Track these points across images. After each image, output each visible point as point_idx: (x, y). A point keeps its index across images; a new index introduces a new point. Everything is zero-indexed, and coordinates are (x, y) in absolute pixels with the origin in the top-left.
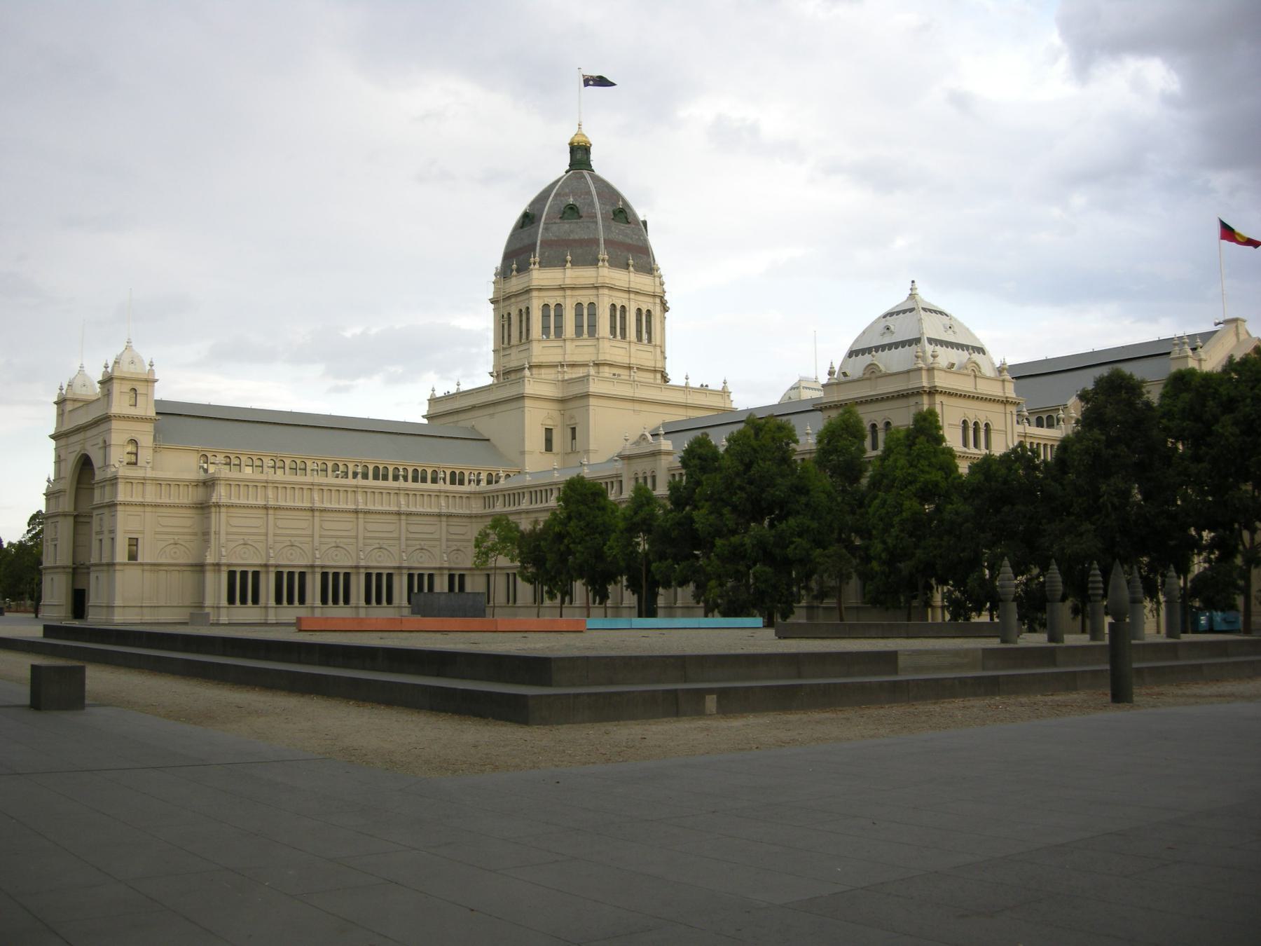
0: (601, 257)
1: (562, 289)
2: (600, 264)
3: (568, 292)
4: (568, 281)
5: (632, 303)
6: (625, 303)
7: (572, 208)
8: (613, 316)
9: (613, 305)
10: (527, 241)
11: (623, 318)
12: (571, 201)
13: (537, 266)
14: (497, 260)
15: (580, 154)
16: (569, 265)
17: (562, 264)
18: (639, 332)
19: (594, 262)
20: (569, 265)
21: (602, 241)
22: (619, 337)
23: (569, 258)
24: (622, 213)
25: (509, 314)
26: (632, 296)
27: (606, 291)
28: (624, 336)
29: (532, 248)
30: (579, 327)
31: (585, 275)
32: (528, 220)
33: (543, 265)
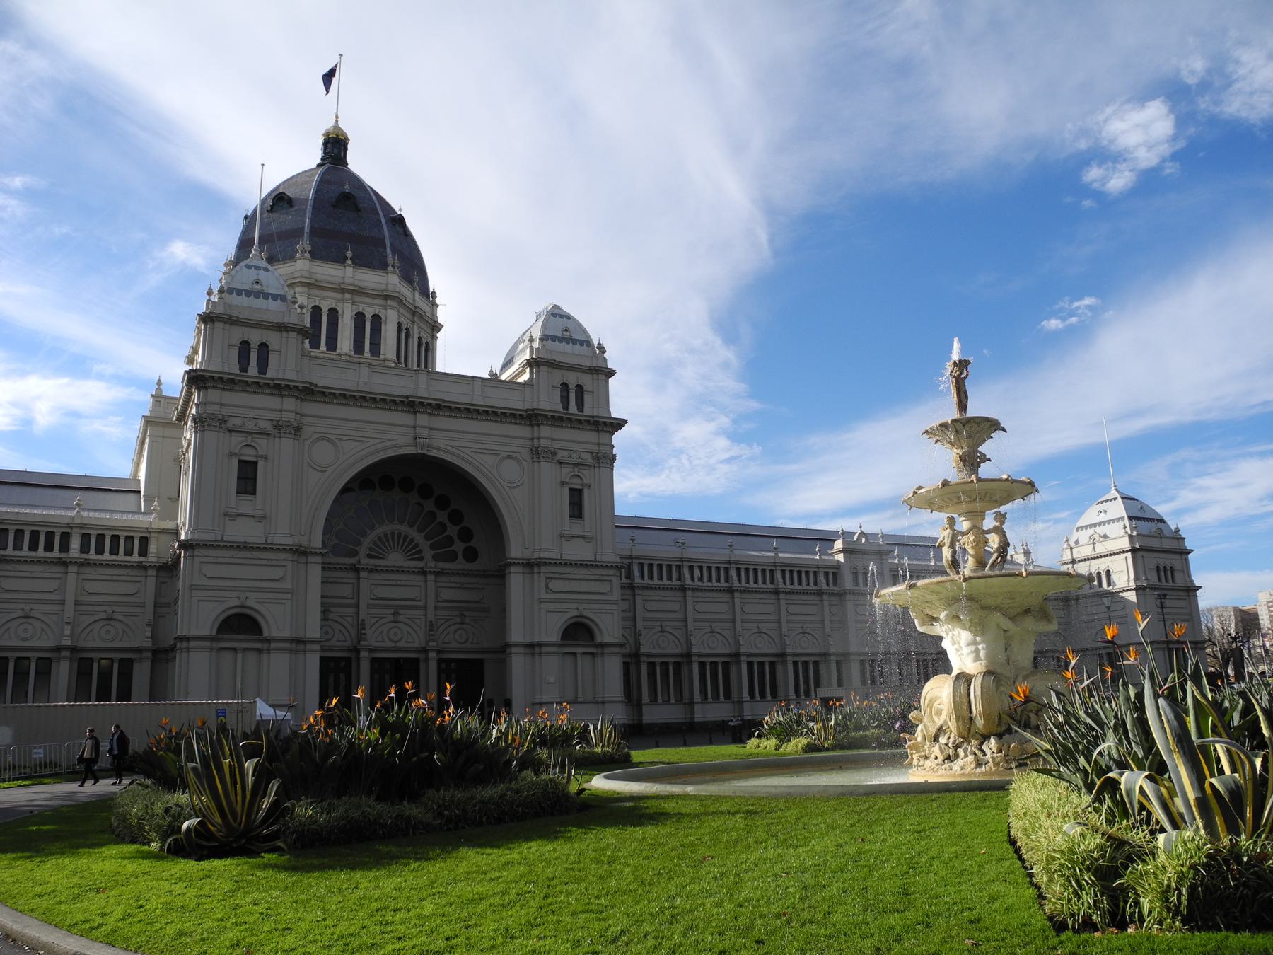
0: (390, 261)
1: (343, 291)
2: (390, 268)
3: (348, 296)
4: (347, 280)
5: (416, 328)
6: (410, 325)
7: (347, 197)
12: (347, 188)
13: (307, 255)
15: (335, 146)
16: (349, 262)
17: (341, 260)
19: (383, 266)
20: (349, 262)
23: (349, 254)
24: (399, 221)
29: (298, 233)
31: (370, 278)
33: (315, 255)
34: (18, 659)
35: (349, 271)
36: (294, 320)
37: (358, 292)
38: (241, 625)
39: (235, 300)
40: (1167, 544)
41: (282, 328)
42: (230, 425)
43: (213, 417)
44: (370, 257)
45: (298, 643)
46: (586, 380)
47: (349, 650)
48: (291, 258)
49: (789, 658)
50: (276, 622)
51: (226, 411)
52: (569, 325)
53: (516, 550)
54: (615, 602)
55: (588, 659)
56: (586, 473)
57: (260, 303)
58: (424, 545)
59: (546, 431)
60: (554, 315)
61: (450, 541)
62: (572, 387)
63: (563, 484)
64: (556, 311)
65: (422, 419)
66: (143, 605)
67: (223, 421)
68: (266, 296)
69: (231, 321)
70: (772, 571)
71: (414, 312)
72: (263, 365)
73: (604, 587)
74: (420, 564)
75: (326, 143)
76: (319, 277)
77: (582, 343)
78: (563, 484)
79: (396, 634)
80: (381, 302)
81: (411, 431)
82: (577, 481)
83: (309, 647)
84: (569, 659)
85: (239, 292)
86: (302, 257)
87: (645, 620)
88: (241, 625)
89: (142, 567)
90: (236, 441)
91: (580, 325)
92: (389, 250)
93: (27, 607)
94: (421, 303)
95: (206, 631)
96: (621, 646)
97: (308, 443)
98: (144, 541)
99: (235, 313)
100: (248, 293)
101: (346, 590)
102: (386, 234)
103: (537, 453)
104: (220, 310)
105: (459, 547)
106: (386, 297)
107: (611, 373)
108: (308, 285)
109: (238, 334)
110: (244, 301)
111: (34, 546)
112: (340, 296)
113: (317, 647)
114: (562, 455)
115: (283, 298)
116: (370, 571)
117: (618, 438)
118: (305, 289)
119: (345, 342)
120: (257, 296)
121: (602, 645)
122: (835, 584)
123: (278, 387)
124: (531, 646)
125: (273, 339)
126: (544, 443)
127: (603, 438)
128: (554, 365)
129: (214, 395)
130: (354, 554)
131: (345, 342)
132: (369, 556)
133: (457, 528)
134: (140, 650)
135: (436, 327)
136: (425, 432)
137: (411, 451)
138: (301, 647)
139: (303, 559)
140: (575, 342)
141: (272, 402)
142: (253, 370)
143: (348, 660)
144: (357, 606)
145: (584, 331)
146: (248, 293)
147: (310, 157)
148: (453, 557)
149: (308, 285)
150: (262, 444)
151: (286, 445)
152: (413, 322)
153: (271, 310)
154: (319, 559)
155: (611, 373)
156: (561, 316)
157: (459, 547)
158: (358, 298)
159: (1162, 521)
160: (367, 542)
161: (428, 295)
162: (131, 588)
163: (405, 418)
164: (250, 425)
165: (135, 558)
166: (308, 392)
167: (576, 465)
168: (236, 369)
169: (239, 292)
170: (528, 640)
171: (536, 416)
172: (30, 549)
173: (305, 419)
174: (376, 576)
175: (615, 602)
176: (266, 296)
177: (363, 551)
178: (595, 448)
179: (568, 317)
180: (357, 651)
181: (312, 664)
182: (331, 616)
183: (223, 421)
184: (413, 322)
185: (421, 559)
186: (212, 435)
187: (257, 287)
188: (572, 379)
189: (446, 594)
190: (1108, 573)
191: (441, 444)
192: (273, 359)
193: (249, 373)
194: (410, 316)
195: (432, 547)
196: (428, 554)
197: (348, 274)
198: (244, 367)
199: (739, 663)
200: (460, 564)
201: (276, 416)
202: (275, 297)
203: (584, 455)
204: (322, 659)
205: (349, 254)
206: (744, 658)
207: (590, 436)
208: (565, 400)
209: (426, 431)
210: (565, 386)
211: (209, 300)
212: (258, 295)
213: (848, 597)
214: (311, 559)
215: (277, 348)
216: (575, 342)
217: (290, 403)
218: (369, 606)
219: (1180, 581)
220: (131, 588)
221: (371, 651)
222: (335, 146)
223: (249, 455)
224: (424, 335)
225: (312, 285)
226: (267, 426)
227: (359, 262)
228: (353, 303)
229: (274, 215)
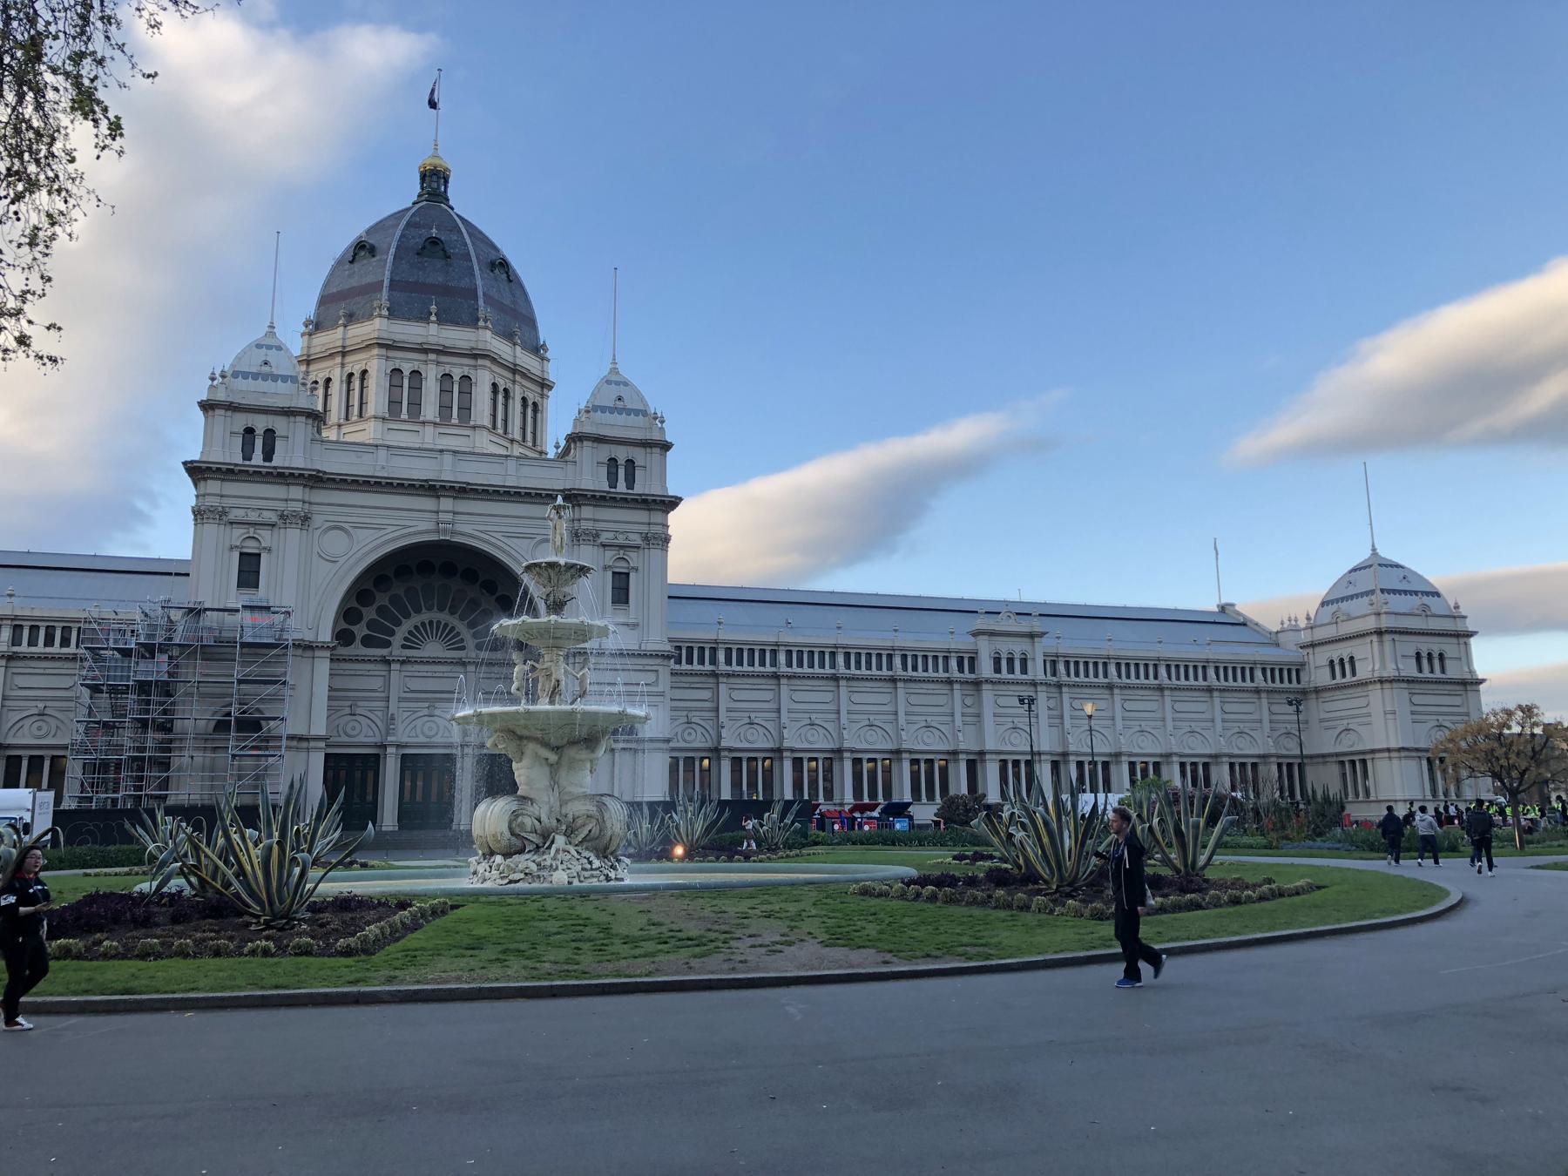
0: (481, 314)
2: (481, 323)
3: (432, 356)
4: (432, 340)
6: (509, 385)
7: (434, 242)
8: (495, 401)
9: (495, 385)
10: (370, 279)
11: (506, 406)
14: (309, 308)
15: (434, 181)
16: (433, 318)
17: (424, 318)
18: (524, 429)
19: (473, 322)
20: (433, 318)
21: (480, 293)
22: (500, 431)
23: (433, 308)
25: (328, 380)
26: (518, 378)
27: (487, 363)
28: (506, 432)
29: (378, 286)
30: (445, 409)
32: (363, 249)
33: (393, 314)
34: (53, 758)
35: (434, 328)
36: (302, 402)
37: (443, 351)
39: (241, 384)
40: (1434, 624)
41: (288, 413)
42: (231, 517)
43: (212, 510)
44: (458, 309)
46: (638, 455)
47: (376, 746)
48: (370, 317)
49: (905, 755)
51: (227, 502)
52: (623, 391)
54: (662, 694)
55: (627, 756)
56: (634, 558)
57: (268, 386)
59: (587, 512)
60: (609, 382)
62: (621, 461)
63: (605, 568)
64: (614, 378)
65: (446, 503)
67: (224, 513)
68: (275, 378)
69: (232, 407)
70: (890, 657)
71: (514, 370)
72: (268, 455)
73: (651, 677)
74: (461, 654)
75: (423, 177)
76: (397, 337)
77: (637, 412)
78: (605, 568)
79: (430, 729)
80: (471, 362)
81: (433, 516)
82: (624, 564)
83: (312, 744)
85: (245, 375)
86: (380, 316)
87: (729, 710)
90: (239, 532)
91: (638, 393)
92: (481, 302)
93: (41, 705)
94: (527, 361)
96: (668, 741)
97: (317, 533)
99: (237, 399)
100: (255, 376)
102: (479, 282)
103: (576, 535)
104: (221, 396)
106: (475, 356)
107: (666, 447)
108: (388, 347)
109: (241, 421)
110: (250, 385)
111: (49, 641)
112: (422, 357)
113: (322, 744)
114: (605, 537)
115: (294, 379)
116: (403, 662)
117: (674, 518)
118: (383, 351)
119: (430, 410)
120: (265, 379)
122: (972, 670)
123: (281, 475)
125: (279, 424)
126: (585, 525)
127: (656, 517)
128: (599, 440)
129: (213, 486)
130: (388, 644)
131: (430, 410)
132: (404, 647)
135: (545, 385)
136: (449, 517)
137: (434, 537)
138: (305, 744)
139: (309, 653)
140: (629, 412)
141: (278, 491)
142: (257, 458)
143: (377, 756)
144: (387, 699)
145: (642, 399)
146: (255, 376)
147: (407, 193)
149: (388, 347)
150: (265, 536)
151: (293, 534)
152: (514, 382)
153: (281, 395)
154: (328, 654)
155: (666, 447)
156: (617, 383)
158: (443, 359)
159: (1437, 594)
160: (401, 632)
161: (537, 349)
163: (427, 503)
164: (253, 517)
166: (316, 480)
167: (621, 547)
168: (238, 459)
169: (245, 375)
171: (576, 496)
172: (46, 645)
173: (315, 508)
174: (409, 667)
175: (662, 694)
176: (275, 378)
177: (397, 640)
178: (644, 529)
179: (626, 384)
180: (384, 747)
181: (317, 763)
182: (358, 711)
183: (224, 513)
184: (514, 382)
185: (463, 648)
186: (211, 529)
187: (266, 369)
188: (622, 454)
190: (1352, 658)
191: (468, 529)
192: (279, 445)
193: (253, 462)
194: (510, 376)
197: (433, 333)
198: (247, 456)
199: (842, 759)
201: (281, 506)
202: (285, 379)
203: (631, 536)
204: (327, 756)
205: (433, 308)
206: (846, 755)
207: (641, 516)
208: (612, 479)
209: (449, 517)
210: (613, 461)
211: (212, 386)
212: (265, 377)
213: (985, 687)
214: (318, 653)
215: (284, 434)
216: (629, 412)
217: (296, 492)
218: (400, 700)
219: (1453, 672)
221: (398, 746)
222: (434, 181)
223: (251, 547)
224: (531, 398)
225: (388, 346)
226: (271, 517)
227: (447, 318)
228: (438, 363)
229: (356, 265)
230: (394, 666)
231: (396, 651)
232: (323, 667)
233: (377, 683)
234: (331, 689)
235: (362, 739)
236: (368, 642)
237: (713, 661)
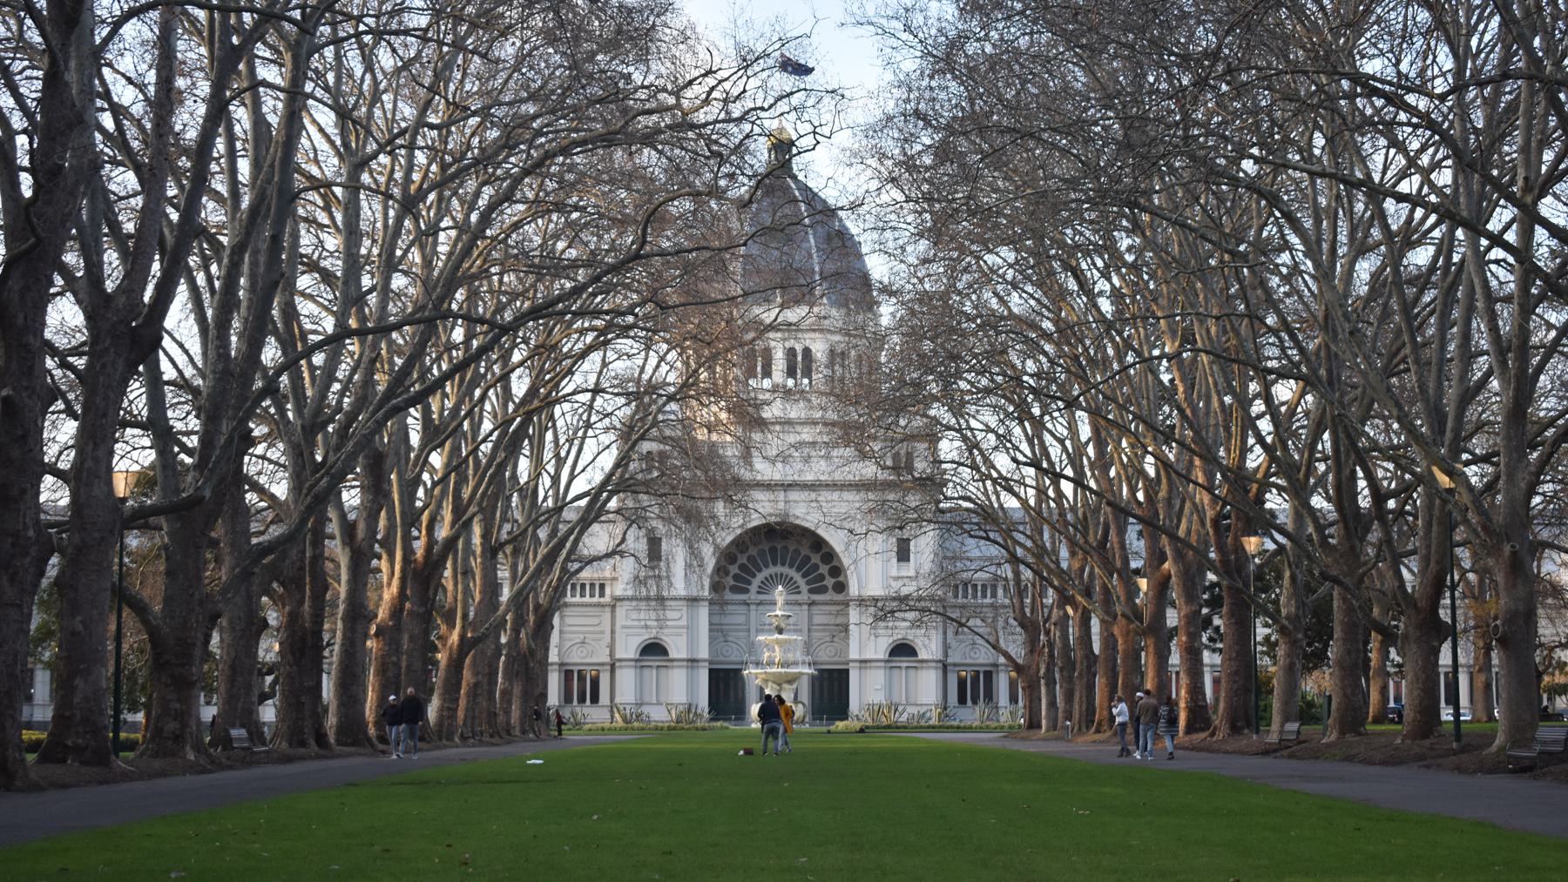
38: (654, 649)
45: (693, 662)
50: (677, 648)
53: (854, 590)
58: (801, 582)
61: (822, 578)
66: (602, 632)
84: (896, 672)
88: (654, 649)
89: (599, 605)
95: (632, 656)
98: (602, 587)
101: (741, 619)
105: (829, 582)
121: (923, 661)
124: (865, 661)
130: (747, 591)
133: (827, 567)
134: (602, 664)
148: (823, 590)
157: (829, 582)
160: (756, 582)
162: (596, 621)
165: (596, 599)
170: (863, 657)
177: (754, 588)
189: (818, 619)
195: (808, 583)
196: (804, 588)
200: (830, 596)
220: (596, 621)
230: (753, 607)
231: (753, 596)
232: (703, 612)
233: (741, 619)
234: (711, 624)
235: (733, 658)
236: (734, 590)
237: (994, 595)
